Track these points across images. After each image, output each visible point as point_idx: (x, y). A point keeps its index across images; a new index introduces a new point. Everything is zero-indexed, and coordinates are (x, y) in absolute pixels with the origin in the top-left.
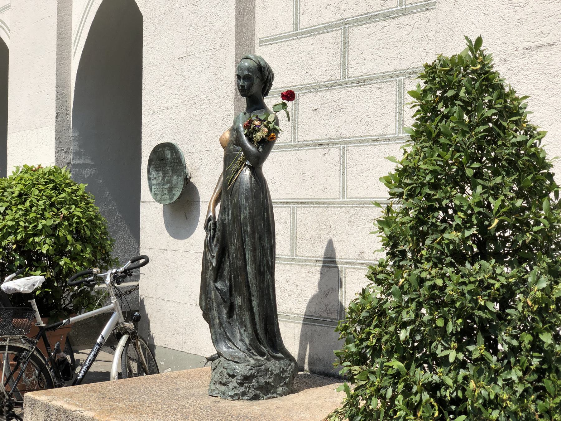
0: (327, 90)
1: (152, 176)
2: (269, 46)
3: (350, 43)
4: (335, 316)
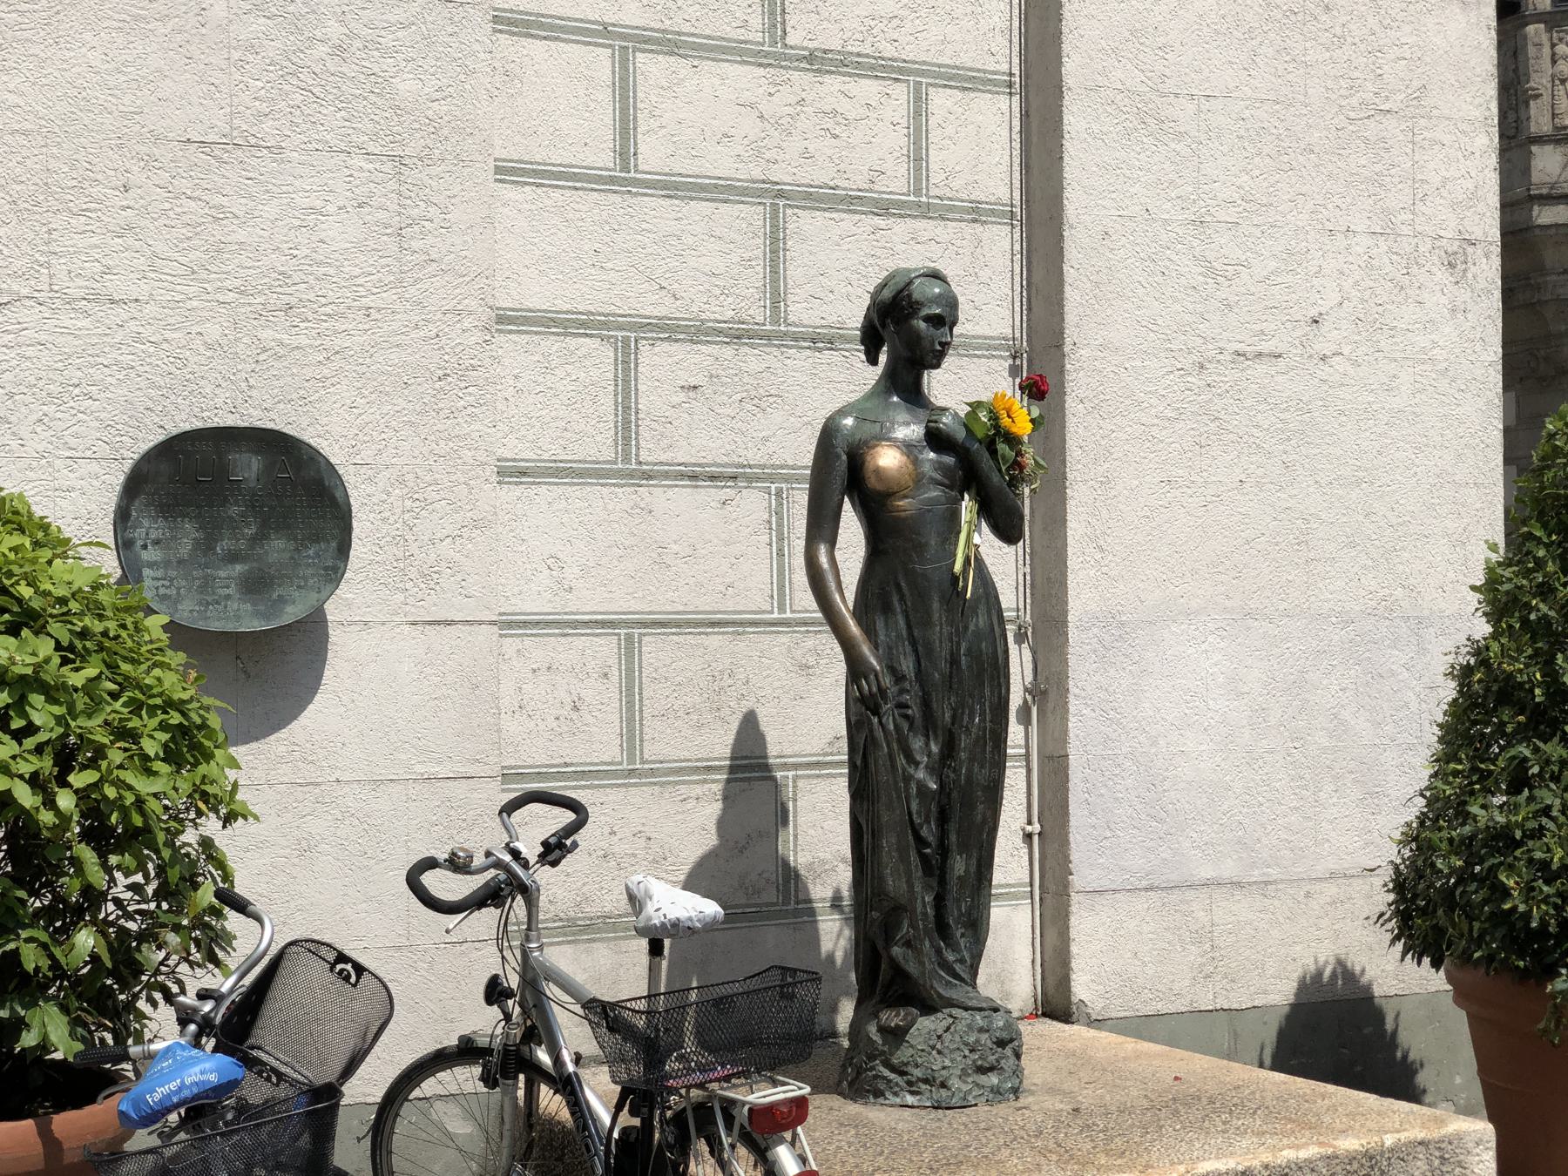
0: (727, 343)
1: (139, 534)
2: (527, 188)
3: (789, 243)
4: (770, 895)
